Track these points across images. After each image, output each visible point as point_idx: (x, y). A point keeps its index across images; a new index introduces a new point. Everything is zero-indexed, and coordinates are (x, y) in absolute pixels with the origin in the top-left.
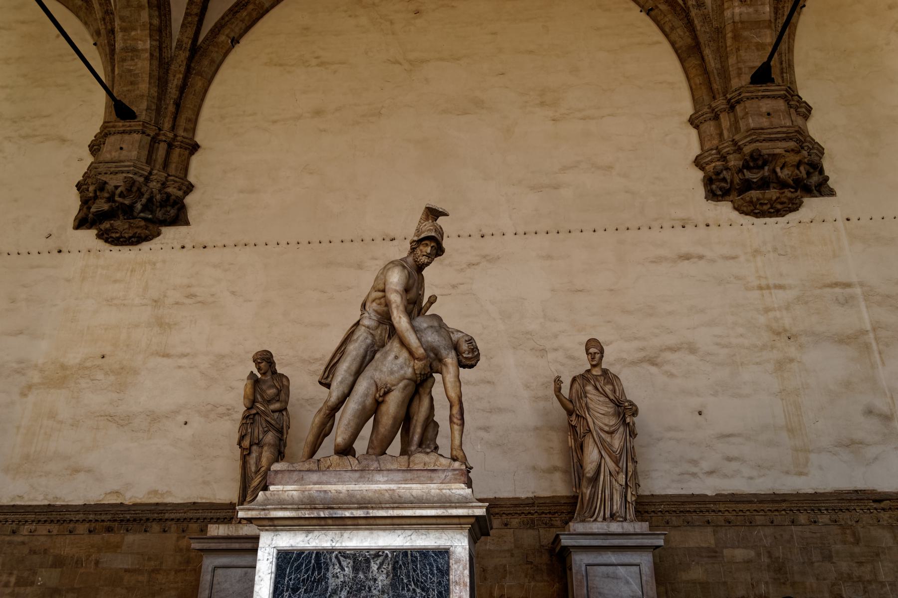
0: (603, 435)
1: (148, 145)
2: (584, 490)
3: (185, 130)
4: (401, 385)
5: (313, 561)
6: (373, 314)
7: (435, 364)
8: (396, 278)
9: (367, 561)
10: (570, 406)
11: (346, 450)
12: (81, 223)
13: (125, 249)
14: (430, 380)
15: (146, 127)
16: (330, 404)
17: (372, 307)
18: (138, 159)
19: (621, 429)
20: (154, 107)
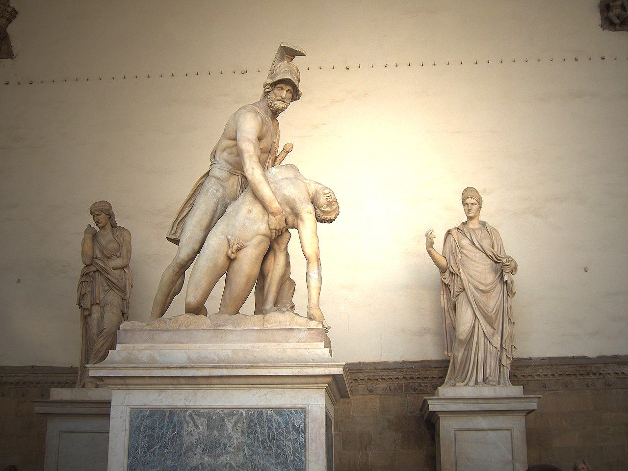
0: (477, 294)
2: (456, 354)
4: (255, 241)
6: (224, 164)
7: (290, 219)
8: (249, 126)
9: (222, 419)
10: (443, 262)
11: (198, 310)
14: (286, 235)
16: (179, 260)
17: (223, 157)
19: (499, 287)
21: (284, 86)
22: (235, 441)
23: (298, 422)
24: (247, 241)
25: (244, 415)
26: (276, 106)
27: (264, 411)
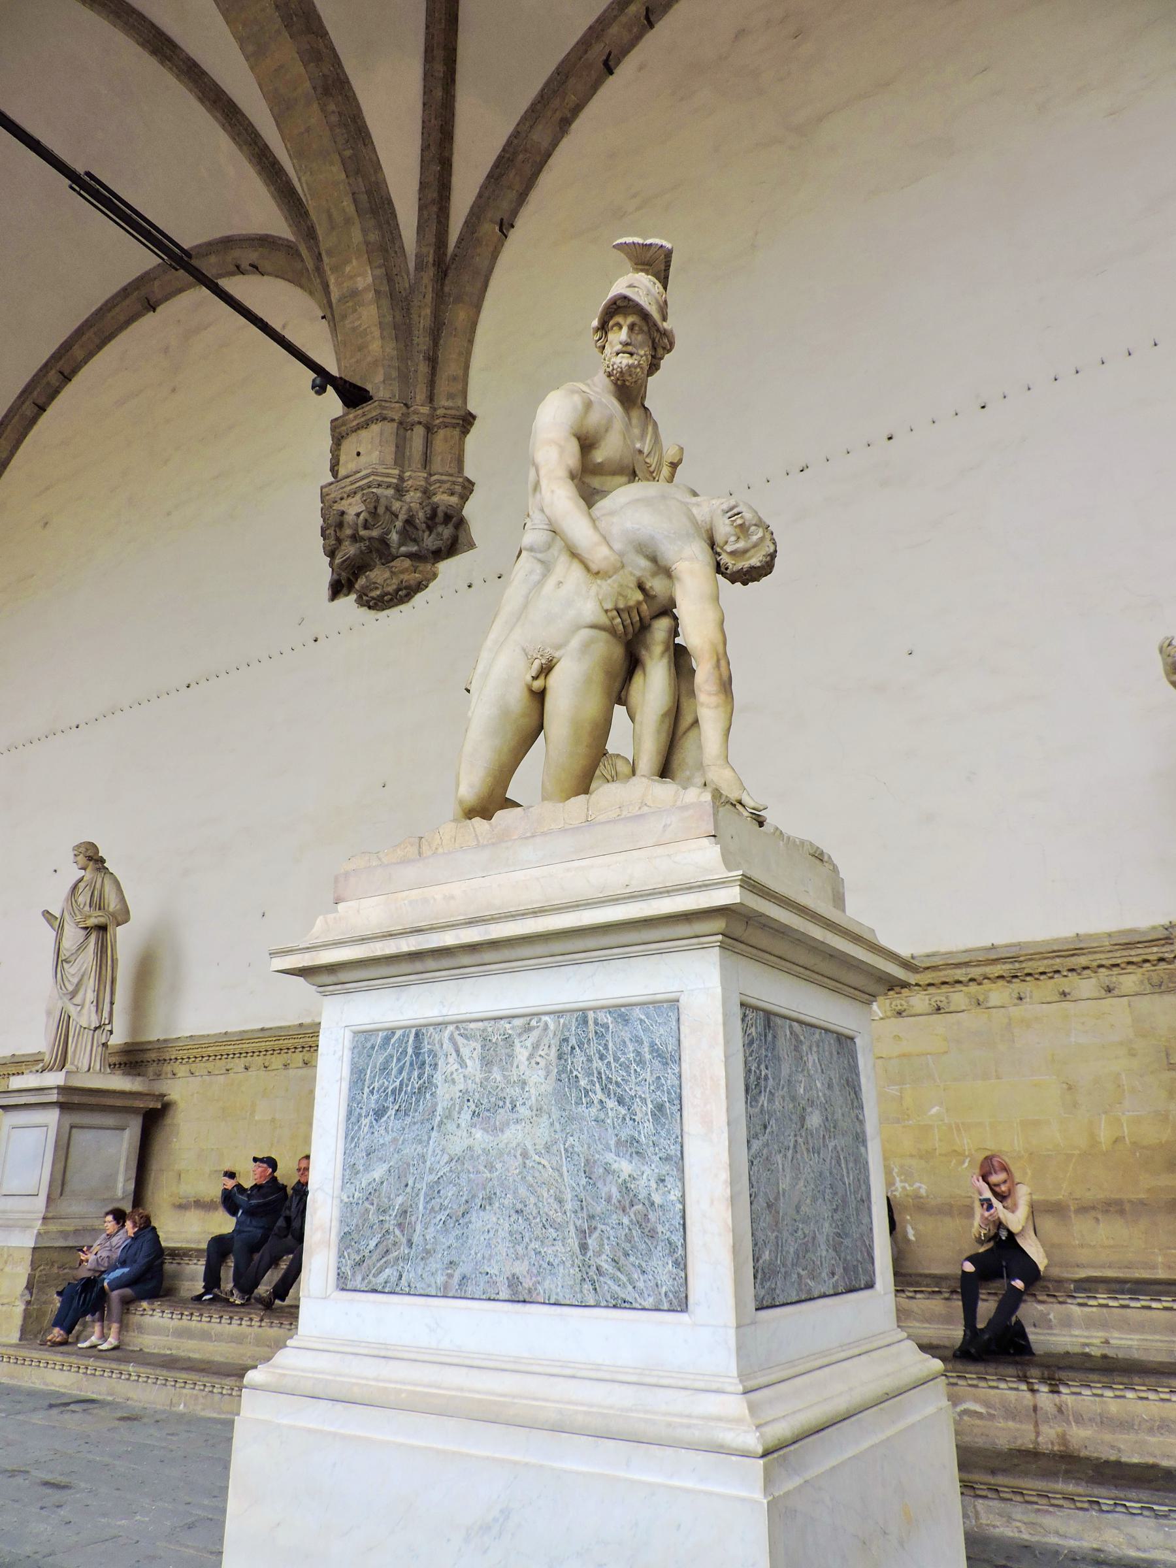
3: (451, 396)
4: (575, 643)
5: (410, 1051)
9: (508, 1039)
12: (338, 589)
13: (394, 612)
15: (384, 408)
18: (382, 463)
20: (395, 374)
21: (619, 319)
22: (533, 1091)
23: (661, 1034)
24: (559, 647)
25: (552, 1026)
27: (591, 1015)
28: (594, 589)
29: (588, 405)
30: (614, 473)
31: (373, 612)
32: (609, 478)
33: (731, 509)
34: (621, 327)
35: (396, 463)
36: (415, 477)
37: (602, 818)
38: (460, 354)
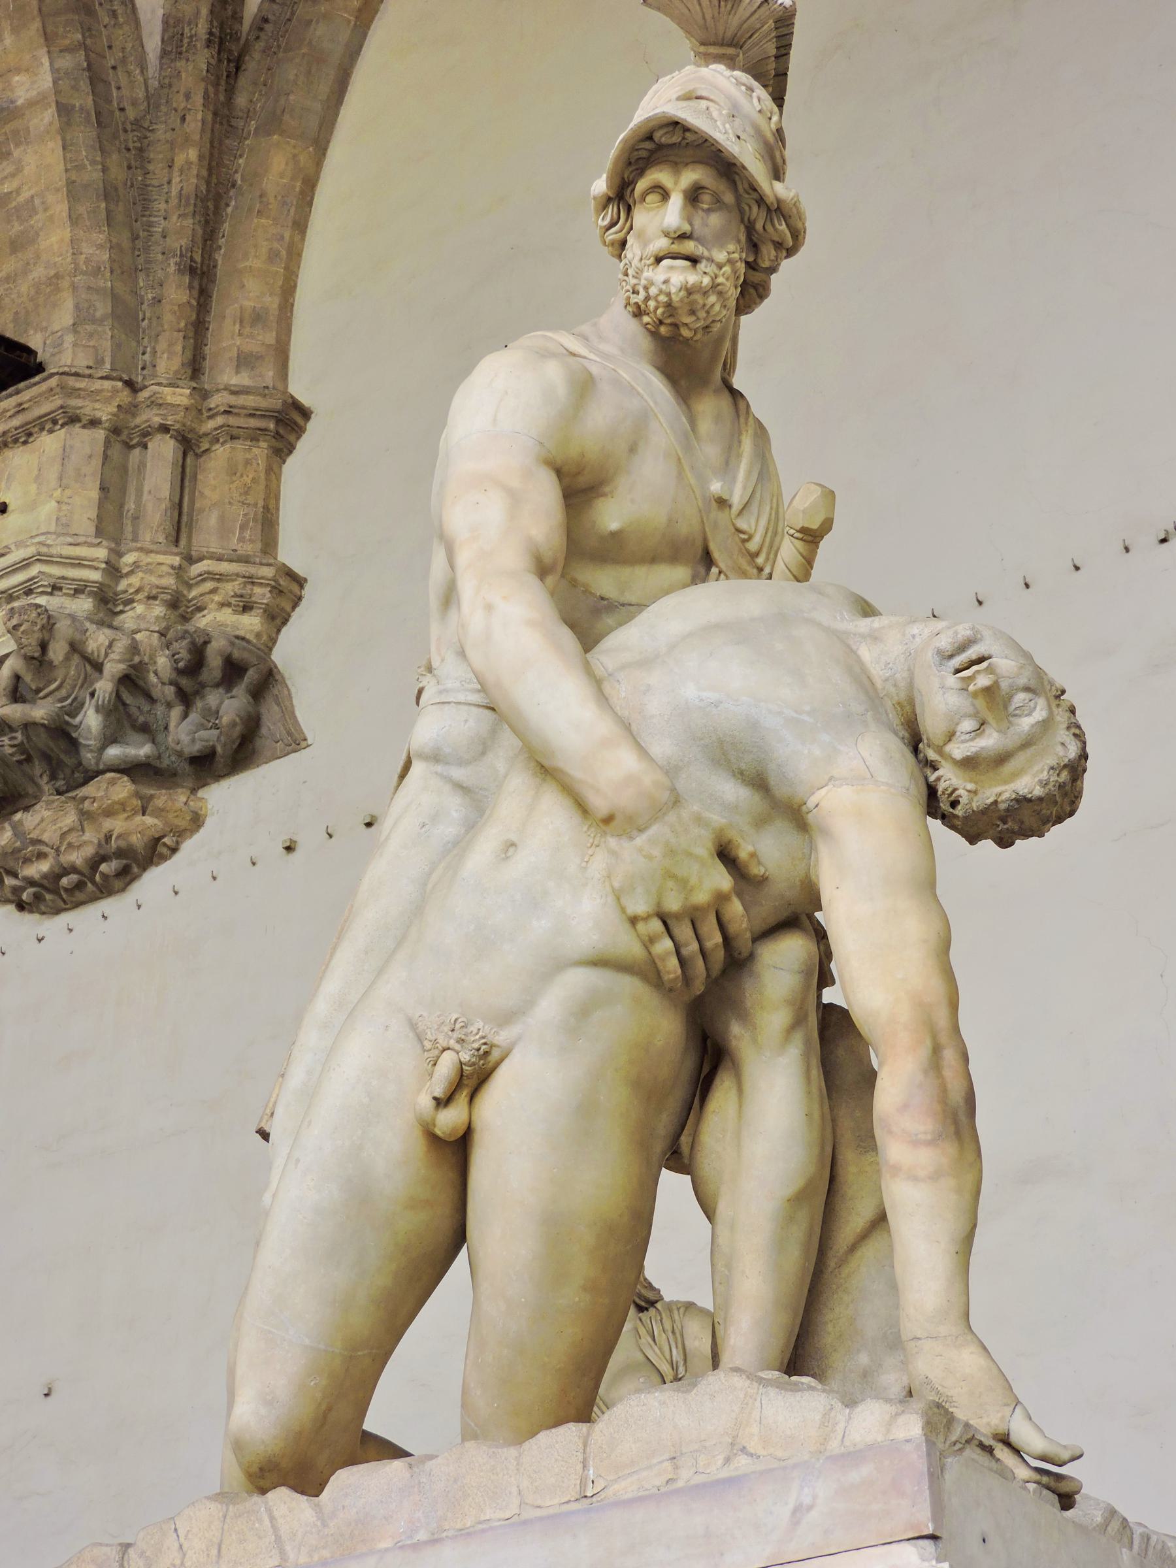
1: (97, 462)
3: (244, 361)
4: (551, 1005)
15: (74, 392)
18: (63, 527)
20: (102, 308)
21: (659, 175)
24: (507, 1018)
26: (653, 291)
28: (599, 863)
29: (584, 387)
30: (653, 559)
31: (28, 918)
32: (640, 571)
33: (963, 648)
34: (665, 195)
35: (99, 532)
36: (150, 566)
37: (626, 1488)
38: (273, 256)
